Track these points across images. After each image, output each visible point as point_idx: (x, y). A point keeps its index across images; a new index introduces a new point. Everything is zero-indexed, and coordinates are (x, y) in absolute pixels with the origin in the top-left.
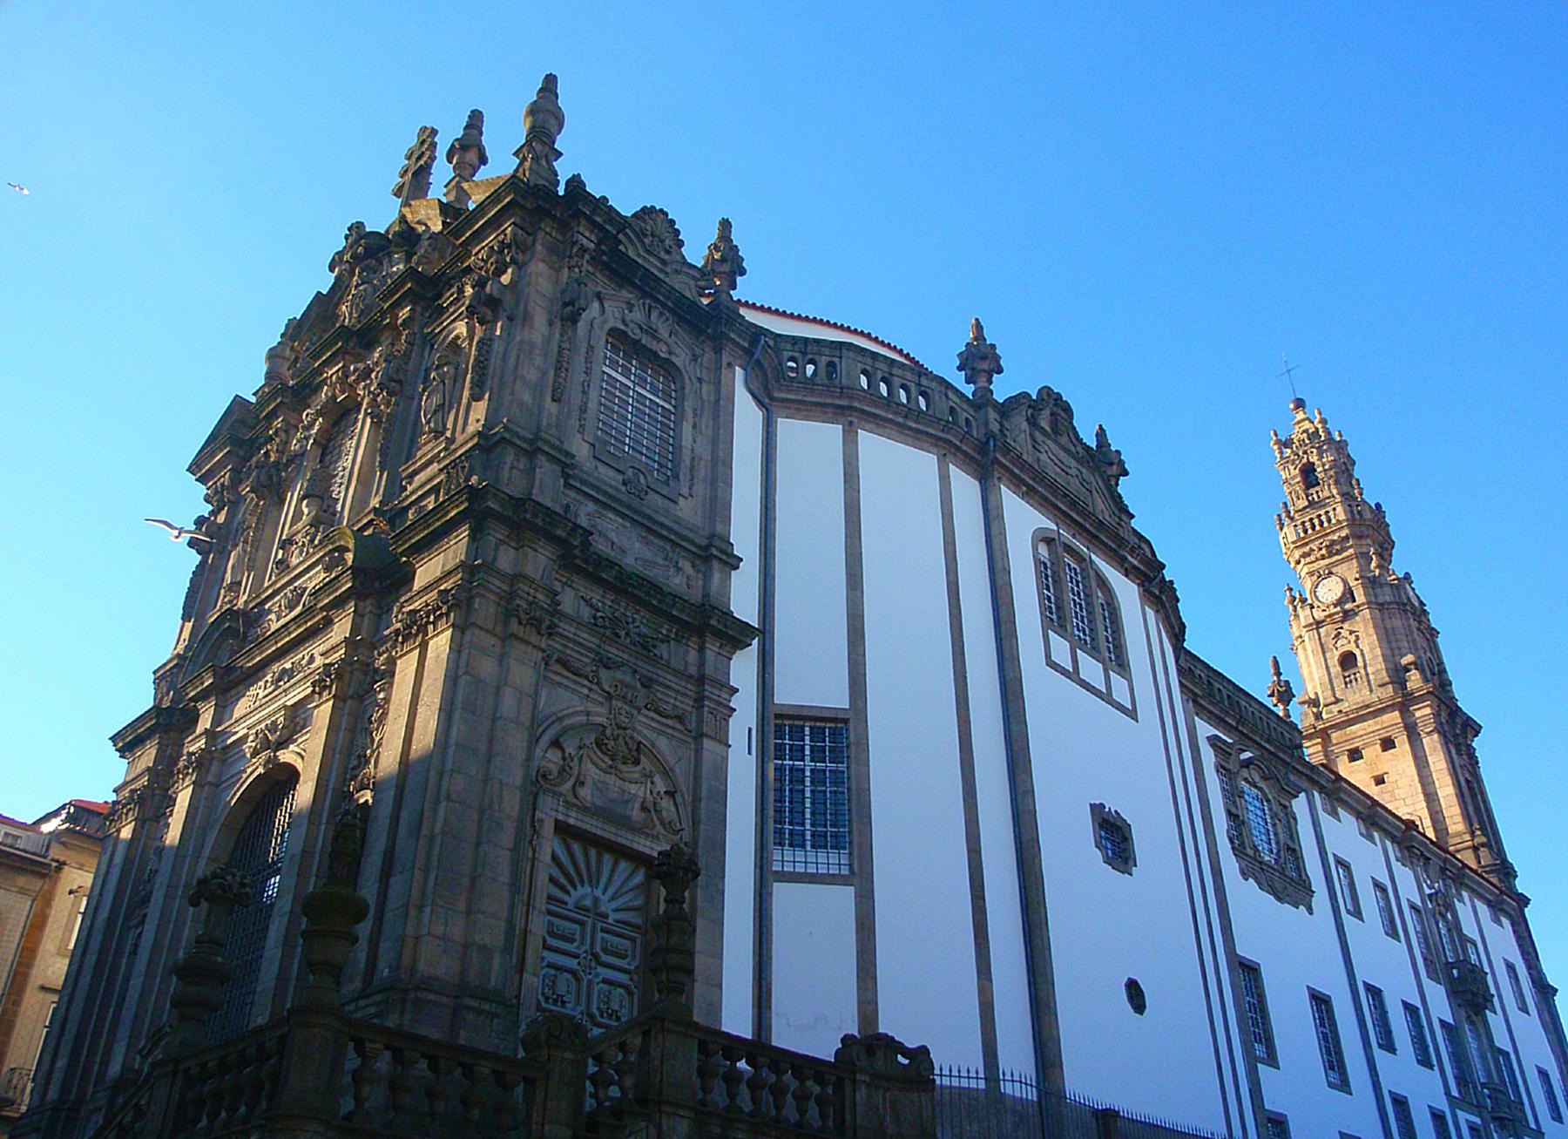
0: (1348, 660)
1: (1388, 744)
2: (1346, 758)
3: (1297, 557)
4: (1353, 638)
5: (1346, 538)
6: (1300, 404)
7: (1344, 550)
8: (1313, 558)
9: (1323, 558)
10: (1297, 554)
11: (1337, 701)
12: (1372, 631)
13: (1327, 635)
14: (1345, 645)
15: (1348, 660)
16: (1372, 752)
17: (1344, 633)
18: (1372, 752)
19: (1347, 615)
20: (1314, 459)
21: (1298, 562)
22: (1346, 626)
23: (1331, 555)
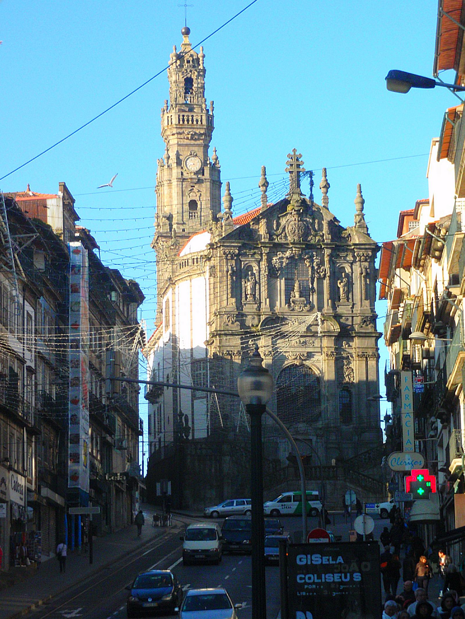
0: (193, 204)
3: (174, 132)
4: (199, 195)
5: (201, 134)
6: (187, 32)
7: (199, 139)
8: (182, 136)
9: (188, 138)
10: (175, 131)
11: (184, 223)
12: (208, 195)
13: (186, 187)
14: (194, 196)
15: (193, 204)
17: (195, 190)
19: (200, 181)
20: (194, 77)
21: (173, 135)
22: (196, 186)
23: (192, 139)
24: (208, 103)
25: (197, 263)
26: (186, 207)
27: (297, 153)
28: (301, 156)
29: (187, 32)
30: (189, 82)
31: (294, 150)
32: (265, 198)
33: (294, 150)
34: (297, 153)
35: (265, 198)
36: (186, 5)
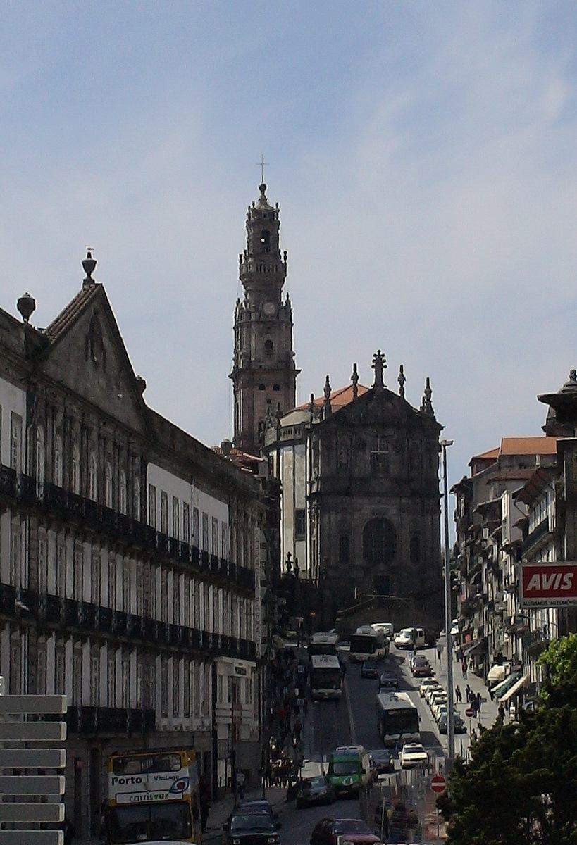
0: (269, 344)
1: (276, 388)
2: (258, 388)
14: (269, 337)
15: (269, 344)
16: (269, 389)
18: (269, 389)
20: (270, 230)
24: (282, 254)
25: (299, 432)
26: (262, 346)
27: (381, 354)
28: (383, 355)
29: (263, 188)
30: (266, 234)
31: (379, 352)
32: (355, 391)
33: (379, 352)
34: (381, 354)
35: (355, 391)
36: (262, 164)
